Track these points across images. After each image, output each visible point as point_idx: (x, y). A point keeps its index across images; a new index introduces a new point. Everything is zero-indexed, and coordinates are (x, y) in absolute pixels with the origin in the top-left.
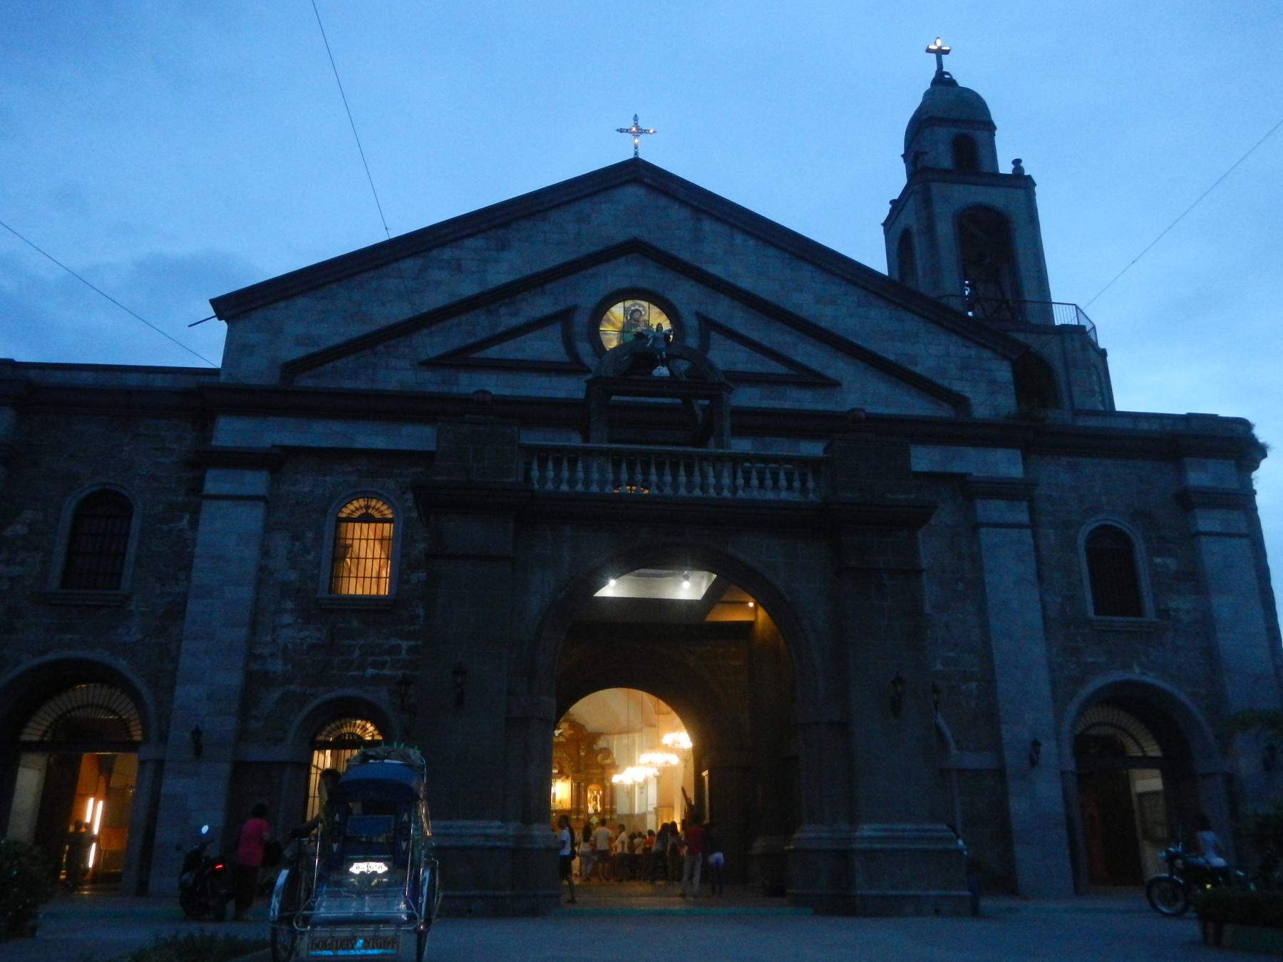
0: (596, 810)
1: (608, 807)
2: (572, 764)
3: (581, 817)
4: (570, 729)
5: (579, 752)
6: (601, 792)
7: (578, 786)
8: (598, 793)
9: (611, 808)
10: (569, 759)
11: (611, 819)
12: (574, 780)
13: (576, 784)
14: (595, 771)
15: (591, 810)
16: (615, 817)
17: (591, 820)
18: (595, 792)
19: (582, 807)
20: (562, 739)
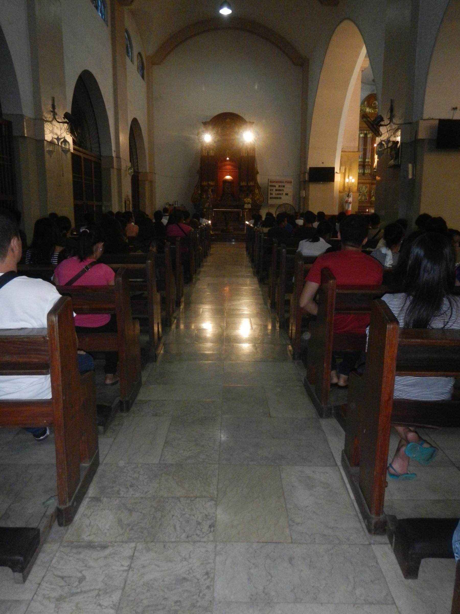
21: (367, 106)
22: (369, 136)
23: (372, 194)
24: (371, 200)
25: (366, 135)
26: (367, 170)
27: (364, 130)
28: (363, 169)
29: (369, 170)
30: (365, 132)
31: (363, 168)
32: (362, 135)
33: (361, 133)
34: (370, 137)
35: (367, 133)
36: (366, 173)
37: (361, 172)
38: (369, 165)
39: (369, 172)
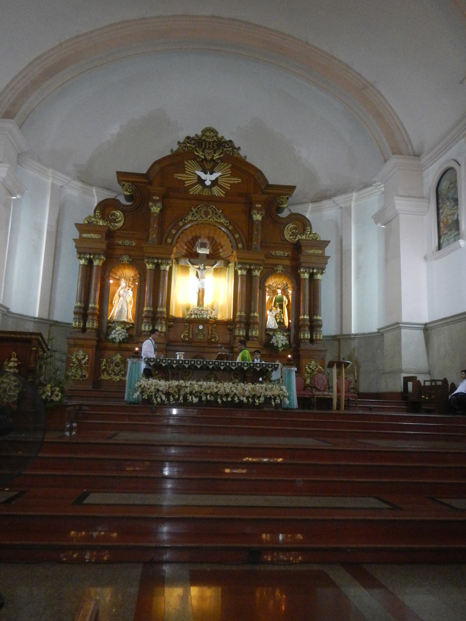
0: (281, 323)
1: (307, 317)
2: (237, 236)
3: (255, 333)
4: (232, 175)
5: (251, 217)
6: (290, 292)
7: (249, 276)
8: (284, 292)
9: (311, 320)
10: (231, 228)
11: (312, 341)
12: (242, 263)
13: (245, 273)
14: (279, 253)
15: (271, 323)
16: (320, 337)
17: (273, 341)
18: (279, 291)
19: (256, 314)
20: (216, 191)
21: (99, 217)
22: (96, 263)
23: (104, 368)
24: (101, 379)
25: (90, 262)
26: (88, 323)
27: (85, 254)
28: (82, 321)
29: (93, 323)
30: (88, 257)
31: (83, 320)
32: (82, 262)
33: (80, 258)
34: (98, 266)
35: (90, 258)
36: (89, 328)
37: (79, 325)
38: (93, 314)
39: (95, 327)
